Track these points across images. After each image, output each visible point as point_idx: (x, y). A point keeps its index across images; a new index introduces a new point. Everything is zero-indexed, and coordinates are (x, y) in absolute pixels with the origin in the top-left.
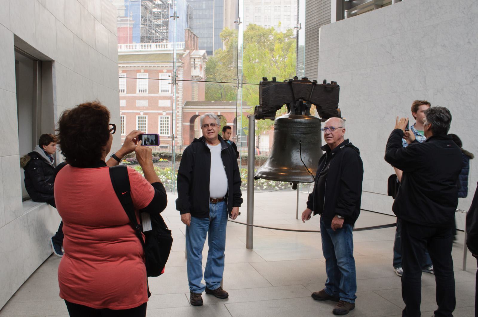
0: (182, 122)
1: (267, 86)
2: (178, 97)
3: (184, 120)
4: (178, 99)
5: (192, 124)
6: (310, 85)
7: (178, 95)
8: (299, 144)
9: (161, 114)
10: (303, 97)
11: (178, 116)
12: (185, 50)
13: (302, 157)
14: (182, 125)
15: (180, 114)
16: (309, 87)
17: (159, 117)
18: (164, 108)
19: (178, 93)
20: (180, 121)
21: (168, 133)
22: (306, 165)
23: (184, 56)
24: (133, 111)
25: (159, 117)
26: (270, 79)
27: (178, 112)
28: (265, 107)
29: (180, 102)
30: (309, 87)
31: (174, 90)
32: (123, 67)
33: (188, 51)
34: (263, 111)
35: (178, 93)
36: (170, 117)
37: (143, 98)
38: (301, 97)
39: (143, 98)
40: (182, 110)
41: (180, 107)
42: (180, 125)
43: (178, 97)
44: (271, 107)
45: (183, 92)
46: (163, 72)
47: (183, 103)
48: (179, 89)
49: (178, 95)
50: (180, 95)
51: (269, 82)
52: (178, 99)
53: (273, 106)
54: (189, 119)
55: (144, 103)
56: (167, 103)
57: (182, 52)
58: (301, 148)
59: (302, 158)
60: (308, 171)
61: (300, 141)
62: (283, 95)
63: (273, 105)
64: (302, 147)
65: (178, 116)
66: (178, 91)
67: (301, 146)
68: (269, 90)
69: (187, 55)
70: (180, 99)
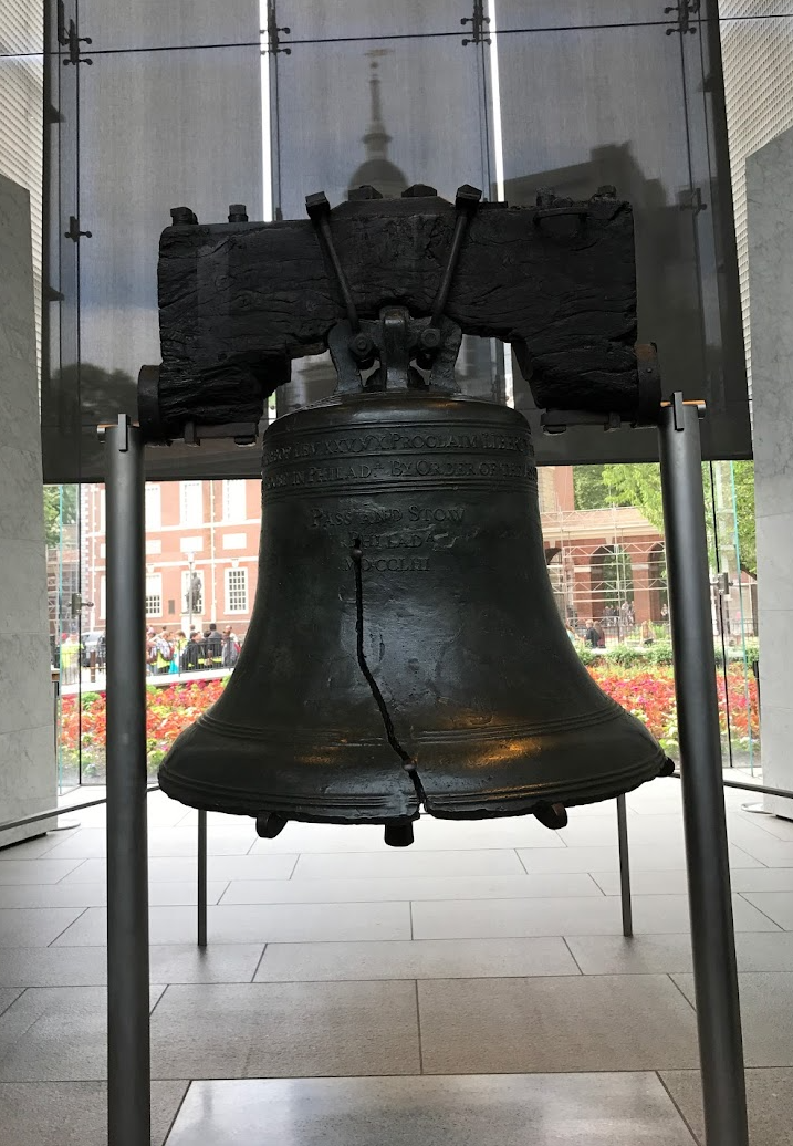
8: (350, 562)
10: (403, 291)
16: (436, 232)
22: (386, 696)
26: (211, 213)
28: (179, 371)
30: (436, 232)
34: (161, 392)
38: (391, 295)
44: (214, 365)
51: (207, 234)
53: (221, 363)
58: (364, 585)
59: (366, 651)
60: (393, 741)
61: (357, 547)
62: (280, 295)
63: (222, 356)
64: (366, 580)
67: (363, 577)
68: (194, 271)
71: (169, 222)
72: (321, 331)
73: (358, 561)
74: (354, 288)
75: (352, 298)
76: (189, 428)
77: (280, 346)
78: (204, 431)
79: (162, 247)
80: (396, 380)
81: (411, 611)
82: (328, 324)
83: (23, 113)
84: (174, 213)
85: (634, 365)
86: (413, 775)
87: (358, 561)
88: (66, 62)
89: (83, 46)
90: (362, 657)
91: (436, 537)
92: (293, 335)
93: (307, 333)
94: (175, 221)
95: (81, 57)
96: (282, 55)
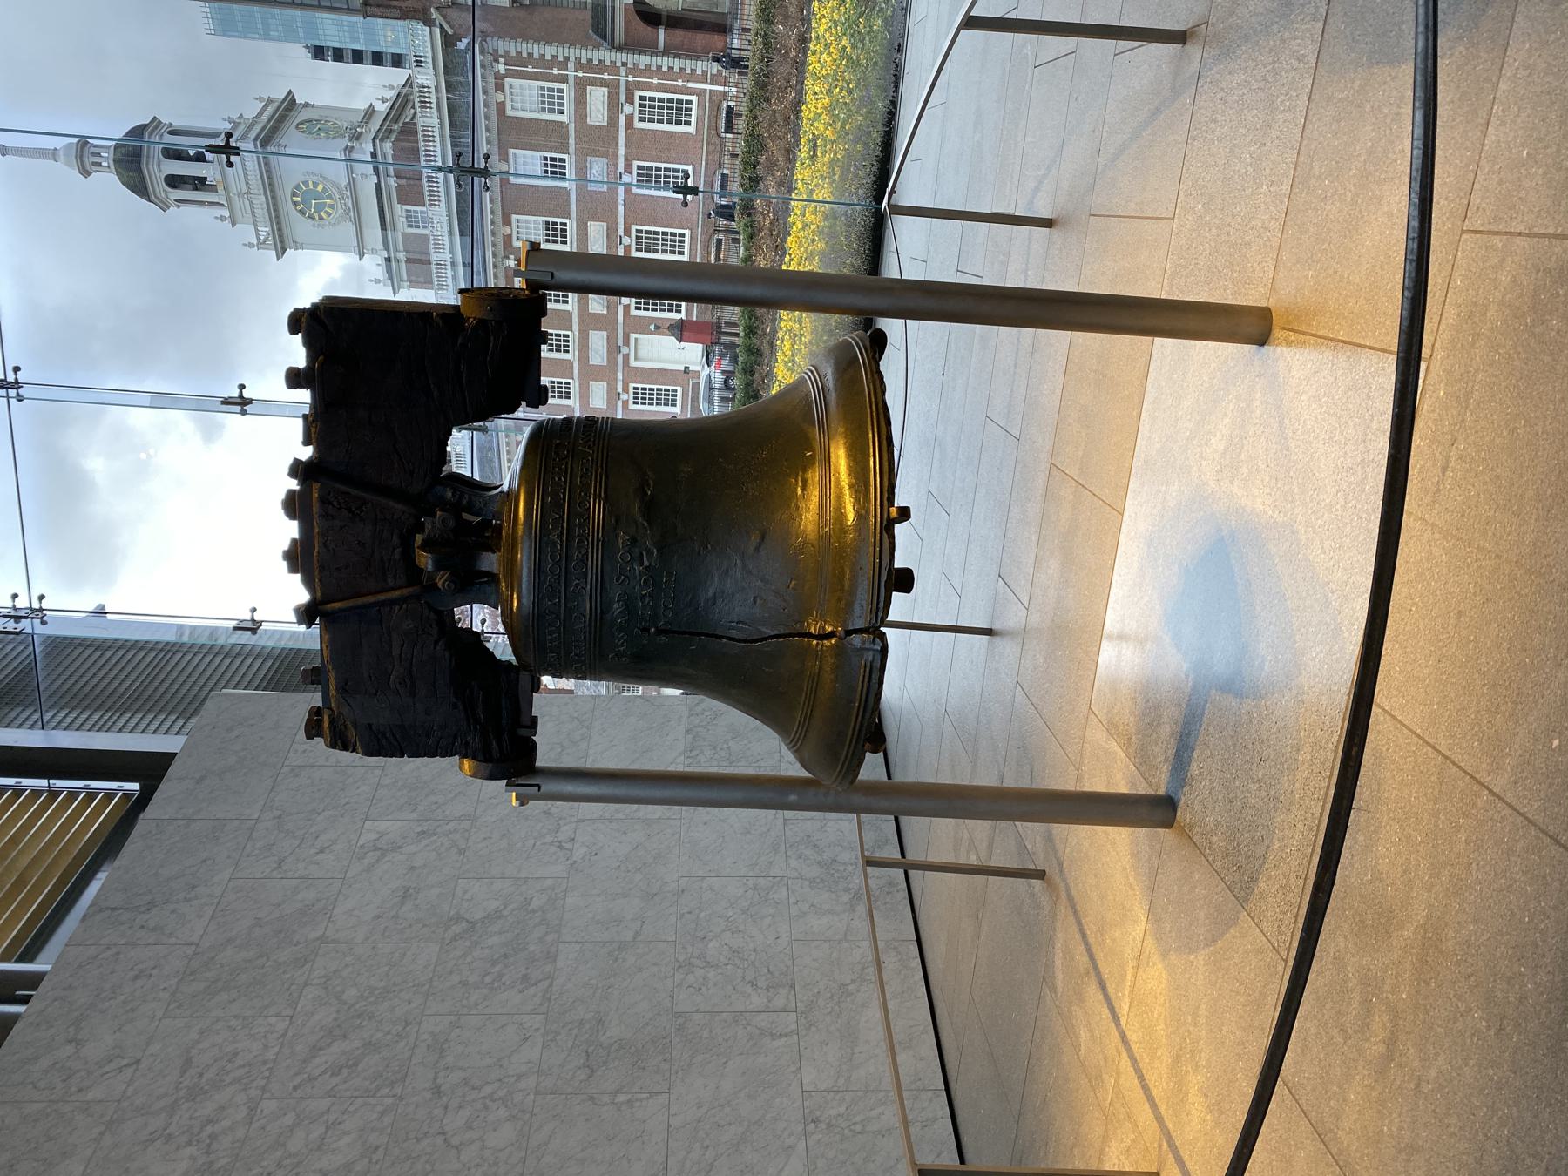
0: (655, 53)
1: (352, 734)
2: (578, 60)
3: (649, 48)
4: (584, 61)
5: (664, 19)
6: (323, 500)
7: (572, 59)
9: (630, 118)
10: (396, 540)
11: (636, 65)
12: (429, 23)
13: (734, 633)
14: (664, 54)
15: (631, 59)
17: (638, 125)
18: (614, 106)
19: (567, 59)
20: (654, 61)
21: (689, 102)
23: (450, 32)
24: (621, 202)
25: (638, 125)
27: (623, 64)
28: (467, 744)
29: (595, 55)
31: (555, 72)
32: (493, 223)
33: (434, 14)
35: (567, 59)
36: (638, 93)
37: (582, 170)
39: (582, 170)
40: (620, 49)
41: (610, 56)
42: (665, 63)
43: (578, 60)
45: (561, 43)
46: (503, 103)
47: (597, 47)
48: (554, 57)
49: (572, 59)
50: (572, 53)
52: (584, 61)
54: (642, 29)
55: (597, 168)
56: (597, 99)
57: (437, 30)
61: (647, 630)
62: (396, 652)
63: (455, 706)
65: (636, 65)
66: (561, 59)
69: (444, 17)
70: (585, 54)
71: (319, 741)
72: (432, 616)
73: (660, 632)
74: (390, 582)
75: (400, 588)
76: (523, 732)
77: (447, 654)
78: (525, 720)
79: (345, 749)
80: (490, 562)
81: (711, 594)
82: (426, 611)
83: (98, 654)
84: (309, 736)
85: (482, 323)
86: (849, 633)
87: (660, 632)
88: (43, 623)
89: (22, 603)
90: (745, 641)
91: (646, 563)
92: (436, 643)
93: (435, 631)
94: (320, 735)
95: (36, 605)
96: (21, 377)
